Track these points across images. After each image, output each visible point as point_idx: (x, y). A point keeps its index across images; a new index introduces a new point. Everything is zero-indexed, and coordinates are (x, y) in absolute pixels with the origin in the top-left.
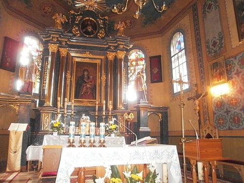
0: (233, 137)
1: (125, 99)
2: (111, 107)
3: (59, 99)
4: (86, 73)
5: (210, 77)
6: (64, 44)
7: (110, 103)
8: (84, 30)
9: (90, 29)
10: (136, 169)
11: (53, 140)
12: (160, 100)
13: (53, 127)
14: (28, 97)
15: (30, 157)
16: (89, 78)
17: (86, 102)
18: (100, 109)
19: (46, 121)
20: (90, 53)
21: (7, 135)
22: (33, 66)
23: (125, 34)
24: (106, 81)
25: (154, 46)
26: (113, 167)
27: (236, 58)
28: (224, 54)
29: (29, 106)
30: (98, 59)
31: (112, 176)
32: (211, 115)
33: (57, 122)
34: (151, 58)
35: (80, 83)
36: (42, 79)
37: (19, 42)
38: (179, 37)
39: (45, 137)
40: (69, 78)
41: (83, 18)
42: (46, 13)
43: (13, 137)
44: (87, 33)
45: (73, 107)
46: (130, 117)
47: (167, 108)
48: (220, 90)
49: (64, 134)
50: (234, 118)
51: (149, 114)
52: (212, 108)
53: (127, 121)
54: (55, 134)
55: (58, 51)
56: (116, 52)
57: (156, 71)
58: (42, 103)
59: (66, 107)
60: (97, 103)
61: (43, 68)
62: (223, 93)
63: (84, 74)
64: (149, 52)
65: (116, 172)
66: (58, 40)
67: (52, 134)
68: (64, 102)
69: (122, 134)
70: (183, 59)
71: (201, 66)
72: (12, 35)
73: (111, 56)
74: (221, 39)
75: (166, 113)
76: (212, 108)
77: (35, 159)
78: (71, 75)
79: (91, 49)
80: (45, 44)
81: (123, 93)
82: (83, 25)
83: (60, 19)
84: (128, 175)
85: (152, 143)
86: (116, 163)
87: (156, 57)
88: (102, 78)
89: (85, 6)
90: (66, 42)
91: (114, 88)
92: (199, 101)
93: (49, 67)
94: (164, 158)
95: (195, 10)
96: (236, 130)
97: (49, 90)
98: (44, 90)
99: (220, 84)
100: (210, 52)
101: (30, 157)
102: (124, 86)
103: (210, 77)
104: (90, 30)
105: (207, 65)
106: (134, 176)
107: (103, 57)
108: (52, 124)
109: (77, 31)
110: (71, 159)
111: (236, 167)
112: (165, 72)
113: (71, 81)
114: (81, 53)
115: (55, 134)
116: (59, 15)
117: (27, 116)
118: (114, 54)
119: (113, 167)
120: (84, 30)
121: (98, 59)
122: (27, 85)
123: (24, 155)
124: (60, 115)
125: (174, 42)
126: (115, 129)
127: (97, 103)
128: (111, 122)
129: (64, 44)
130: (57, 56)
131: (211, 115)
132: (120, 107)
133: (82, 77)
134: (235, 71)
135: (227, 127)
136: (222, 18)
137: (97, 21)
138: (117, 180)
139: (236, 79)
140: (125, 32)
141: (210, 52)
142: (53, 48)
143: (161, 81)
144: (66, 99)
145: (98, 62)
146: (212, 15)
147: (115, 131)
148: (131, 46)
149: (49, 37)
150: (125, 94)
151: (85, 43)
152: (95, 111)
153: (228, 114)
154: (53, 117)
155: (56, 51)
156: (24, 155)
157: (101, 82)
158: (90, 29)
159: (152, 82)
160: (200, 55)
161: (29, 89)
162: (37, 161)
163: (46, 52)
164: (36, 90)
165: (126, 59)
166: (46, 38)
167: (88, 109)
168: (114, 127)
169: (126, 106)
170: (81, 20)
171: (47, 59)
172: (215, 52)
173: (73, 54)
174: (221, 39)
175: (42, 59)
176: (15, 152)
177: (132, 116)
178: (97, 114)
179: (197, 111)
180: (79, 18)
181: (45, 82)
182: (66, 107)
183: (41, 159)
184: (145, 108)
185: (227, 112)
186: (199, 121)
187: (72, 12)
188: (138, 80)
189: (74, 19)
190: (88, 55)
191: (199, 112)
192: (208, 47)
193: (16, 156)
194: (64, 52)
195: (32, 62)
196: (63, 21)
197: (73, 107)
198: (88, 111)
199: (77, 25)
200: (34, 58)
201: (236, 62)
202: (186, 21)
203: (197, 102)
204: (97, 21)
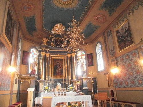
0: (121, 91)
1: (76, 74)
2: (70, 79)
3: (47, 76)
4: (58, 64)
5: (111, 64)
6: (47, 51)
7: (70, 77)
8: (56, 44)
9: (59, 43)
10: (76, 103)
11: (46, 95)
12: (92, 74)
13: (45, 89)
14: (34, 76)
15: (36, 103)
16: (59, 66)
17: (59, 77)
18: (65, 80)
19: (42, 87)
20: (60, 54)
21: (26, 93)
22: (35, 63)
24: (68, 67)
25: (89, 48)
26: (69, 103)
27: (119, 58)
28: (115, 56)
29: (34, 80)
30: (63, 57)
31: (68, 105)
32: (113, 81)
33: (47, 87)
34: (88, 54)
35: (56, 68)
36: (39, 68)
37: (28, 52)
38: (99, 46)
39: (42, 93)
40: (51, 67)
41: (55, 38)
42: (39, 37)
43: (29, 93)
44: (57, 45)
45: (53, 79)
46: (78, 83)
47: (96, 78)
48: (115, 71)
49: (50, 92)
50: (120, 83)
51: (87, 81)
52: (113, 78)
53: (77, 85)
54: (46, 92)
55: (45, 55)
56: (71, 53)
57: (90, 60)
58: (39, 79)
59: (50, 80)
60: (64, 77)
62: (116, 73)
63: (57, 64)
64: (87, 52)
65: (69, 104)
66: (45, 50)
67: (45, 92)
68: (49, 77)
69: (75, 91)
70: (101, 56)
71: (108, 60)
72: (26, 50)
73: (69, 56)
74: (114, 49)
75: (96, 80)
76: (113, 78)
77: (38, 103)
78: (51, 65)
79: (60, 53)
80: (40, 52)
81: (75, 72)
82: (56, 42)
83: (45, 40)
84: (73, 104)
85: (83, 94)
86: (70, 101)
87: (90, 54)
88: (65, 66)
89: (56, 33)
90: (48, 50)
91: (71, 68)
92: (108, 75)
93: (42, 61)
94: (87, 99)
95: (104, 35)
96: (140, 87)
97: (42, 70)
98: (40, 73)
99: (114, 68)
100: (111, 54)
101: (36, 103)
102: (75, 69)
103: (111, 64)
104: (59, 43)
105: (110, 59)
106: (75, 105)
107: (65, 56)
108: (45, 88)
109: (53, 44)
110: (56, 100)
111: (120, 103)
112: (94, 61)
113: (51, 68)
114: (55, 55)
115: (46, 92)
116: (45, 38)
117: (33, 84)
118: (70, 54)
119: (69, 103)
120: (56, 44)
121: (63, 57)
122: (33, 71)
123: (34, 102)
124: (48, 84)
125: (97, 47)
126: (72, 89)
127: (64, 77)
128: (70, 86)
129: (47, 51)
130: (45, 58)
131: (113, 81)
132: (74, 78)
133: (56, 66)
134: (119, 63)
135: (129, 86)
136: (113, 41)
137: (62, 39)
138: (70, 106)
139: (120, 66)
141: (111, 54)
142: (43, 54)
143: (93, 66)
144: (50, 77)
145: (63, 58)
146: (110, 38)
147: (72, 90)
148: (78, 50)
149: (41, 48)
150: (76, 73)
151: (57, 50)
152: (63, 81)
153: (129, 80)
154: (45, 84)
156: (34, 102)
157: (65, 68)
158: (59, 43)
159: (89, 66)
160: (107, 55)
161: (34, 73)
162: (39, 104)
163: (40, 55)
164: (36, 73)
165: (76, 56)
166: (40, 49)
167: (60, 80)
168: (71, 88)
169: (77, 78)
170: (54, 39)
171: (41, 58)
172: (112, 54)
173: (51, 55)
174: (114, 49)
175: (38, 59)
176: (30, 100)
177: (79, 83)
178: (64, 82)
179: (107, 80)
180: (53, 38)
181: (40, 69)
182: (50, 80)
183: (41, 103)
184: (85, 79)
185: (118, 80)
186: (109, 84)
187: (51, 36)
188: (82, 66)
189: (51, 39)
190: (58, 55)
191: (108, 80)
192: (110, 52)
193: (30, 102)
194: (48, 56)
195: (35, 61)
196: (47, 41)
197: (53, 79)
198: (60, 81)
199: (53, 42)
200: (35, 58)
201: (119, 59)
202: (101, 39)
203: (107, 76)
204: (62, 39)
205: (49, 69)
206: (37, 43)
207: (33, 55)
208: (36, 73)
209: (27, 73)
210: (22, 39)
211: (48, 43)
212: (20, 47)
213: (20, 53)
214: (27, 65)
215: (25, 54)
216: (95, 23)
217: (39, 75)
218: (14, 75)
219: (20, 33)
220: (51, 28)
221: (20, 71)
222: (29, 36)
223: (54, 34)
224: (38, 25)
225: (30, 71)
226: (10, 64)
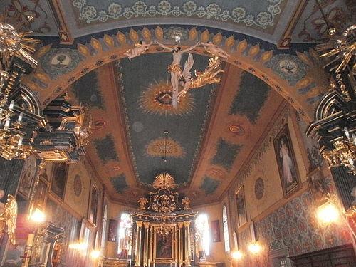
23: (190, 207)
36: (133, 245)
55: (143, 226)
61: (133, 237)
80: (135, 219)
83: (143, 202)
88: (175, 242)
130: (143, 228)
140: (190, 206)
142: (139, 225)
155: (141, 226)
163: (135, 225)
164: (130, 253)
165: (192, 226)
187: (151, 193)
189: (153, 199)
194: (147, 227)
199: (156, 202)
205: (149, 247)
206: (131, 206)
207: (126, 221)
208: (130, 253)
209: (115, 255)
210: (108, 202)
211: (146, 206)
212: (105, 217)
213: (105, 224)
214: (116, 241)
215: (113, 225)
216: (213, 177)
217: (133, 257)
218: (98, 261)
219: (105, 197)
220: (153, 179)
221: (105, 254)
222: (119, 196)
223: (157, 190)
224: (130, 180)
225: (119, 251)
226: (94, 248)
